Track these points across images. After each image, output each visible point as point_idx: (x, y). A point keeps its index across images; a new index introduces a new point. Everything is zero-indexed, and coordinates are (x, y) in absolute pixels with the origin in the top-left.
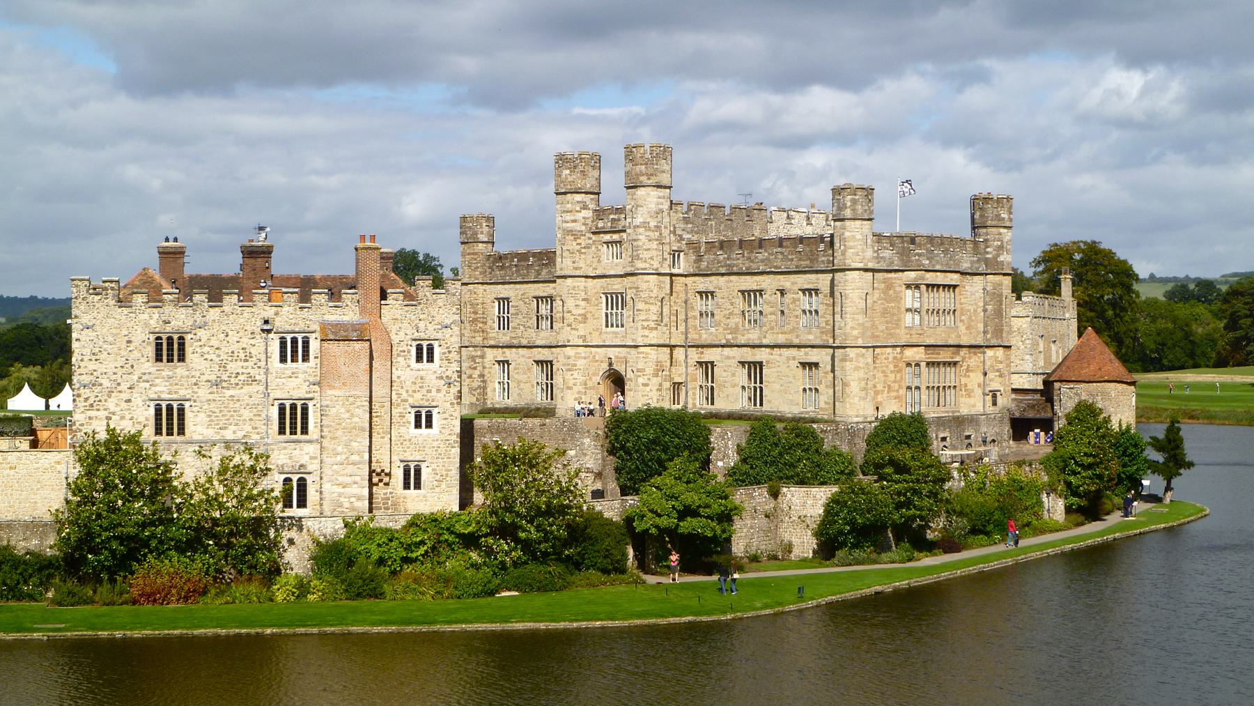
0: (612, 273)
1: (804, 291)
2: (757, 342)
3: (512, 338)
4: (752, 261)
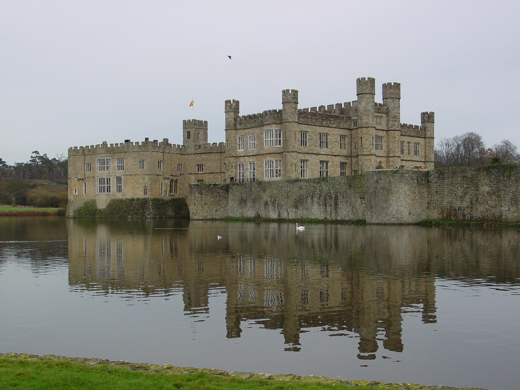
3: (309, 150)
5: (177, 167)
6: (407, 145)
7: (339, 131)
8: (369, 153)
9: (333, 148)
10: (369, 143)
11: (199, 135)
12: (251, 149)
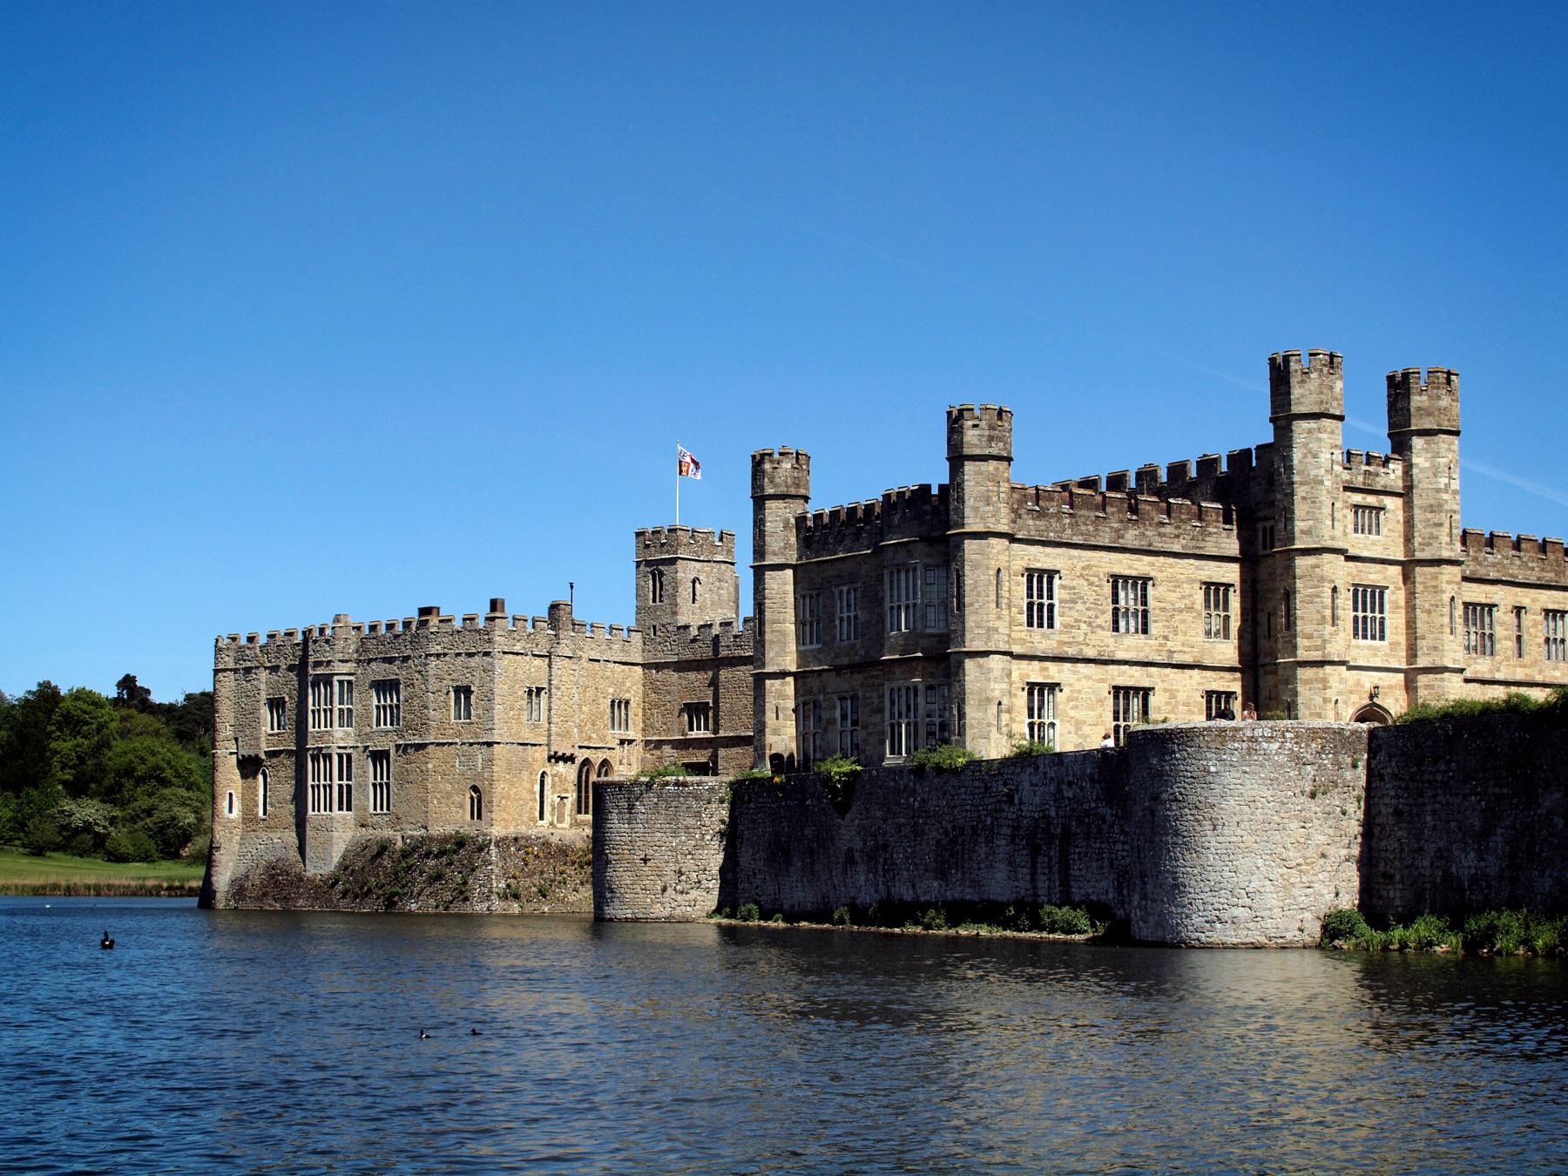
0: (1365, 554)
1: (1547, 611)
2: (1488, 676)
3: (1065, 643)
4: (1480, 564)
5: (609, 711)
6: (1511, 619)
7: (1197, 568)
8: (1315, 655)
9: (1171, 635)
10: (1318, 612)
11: (697, 585)
12: (843, 643)
